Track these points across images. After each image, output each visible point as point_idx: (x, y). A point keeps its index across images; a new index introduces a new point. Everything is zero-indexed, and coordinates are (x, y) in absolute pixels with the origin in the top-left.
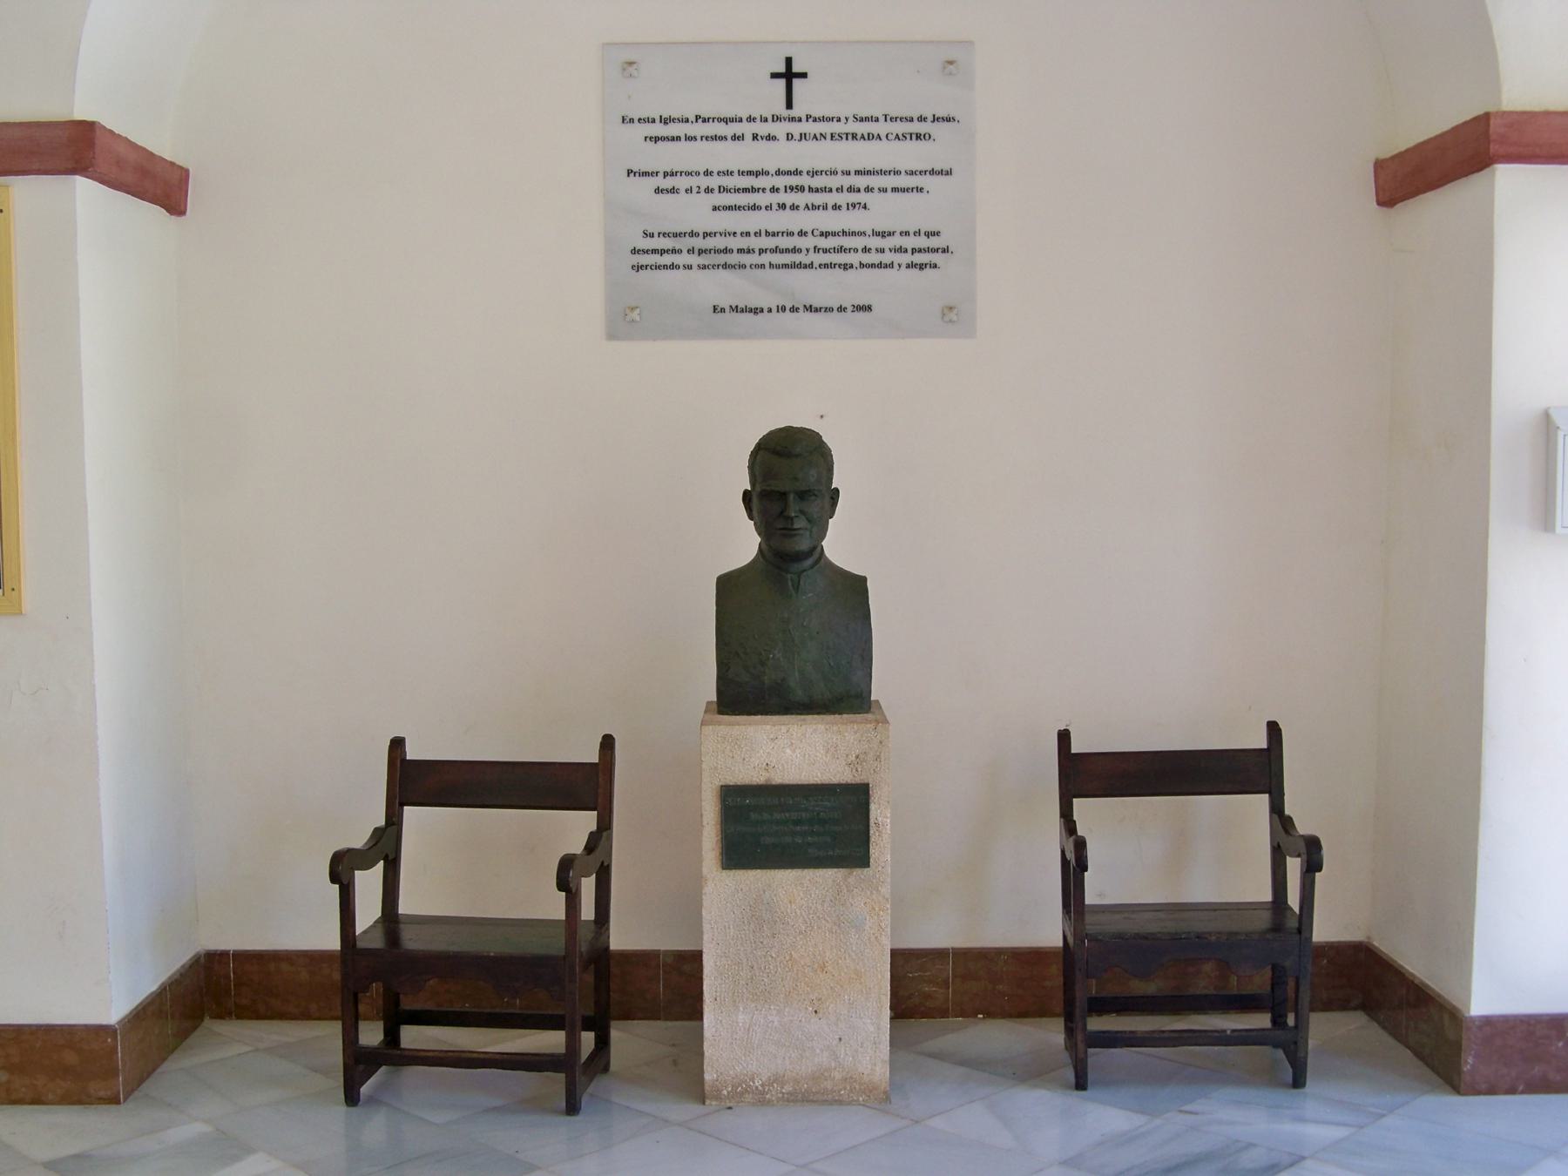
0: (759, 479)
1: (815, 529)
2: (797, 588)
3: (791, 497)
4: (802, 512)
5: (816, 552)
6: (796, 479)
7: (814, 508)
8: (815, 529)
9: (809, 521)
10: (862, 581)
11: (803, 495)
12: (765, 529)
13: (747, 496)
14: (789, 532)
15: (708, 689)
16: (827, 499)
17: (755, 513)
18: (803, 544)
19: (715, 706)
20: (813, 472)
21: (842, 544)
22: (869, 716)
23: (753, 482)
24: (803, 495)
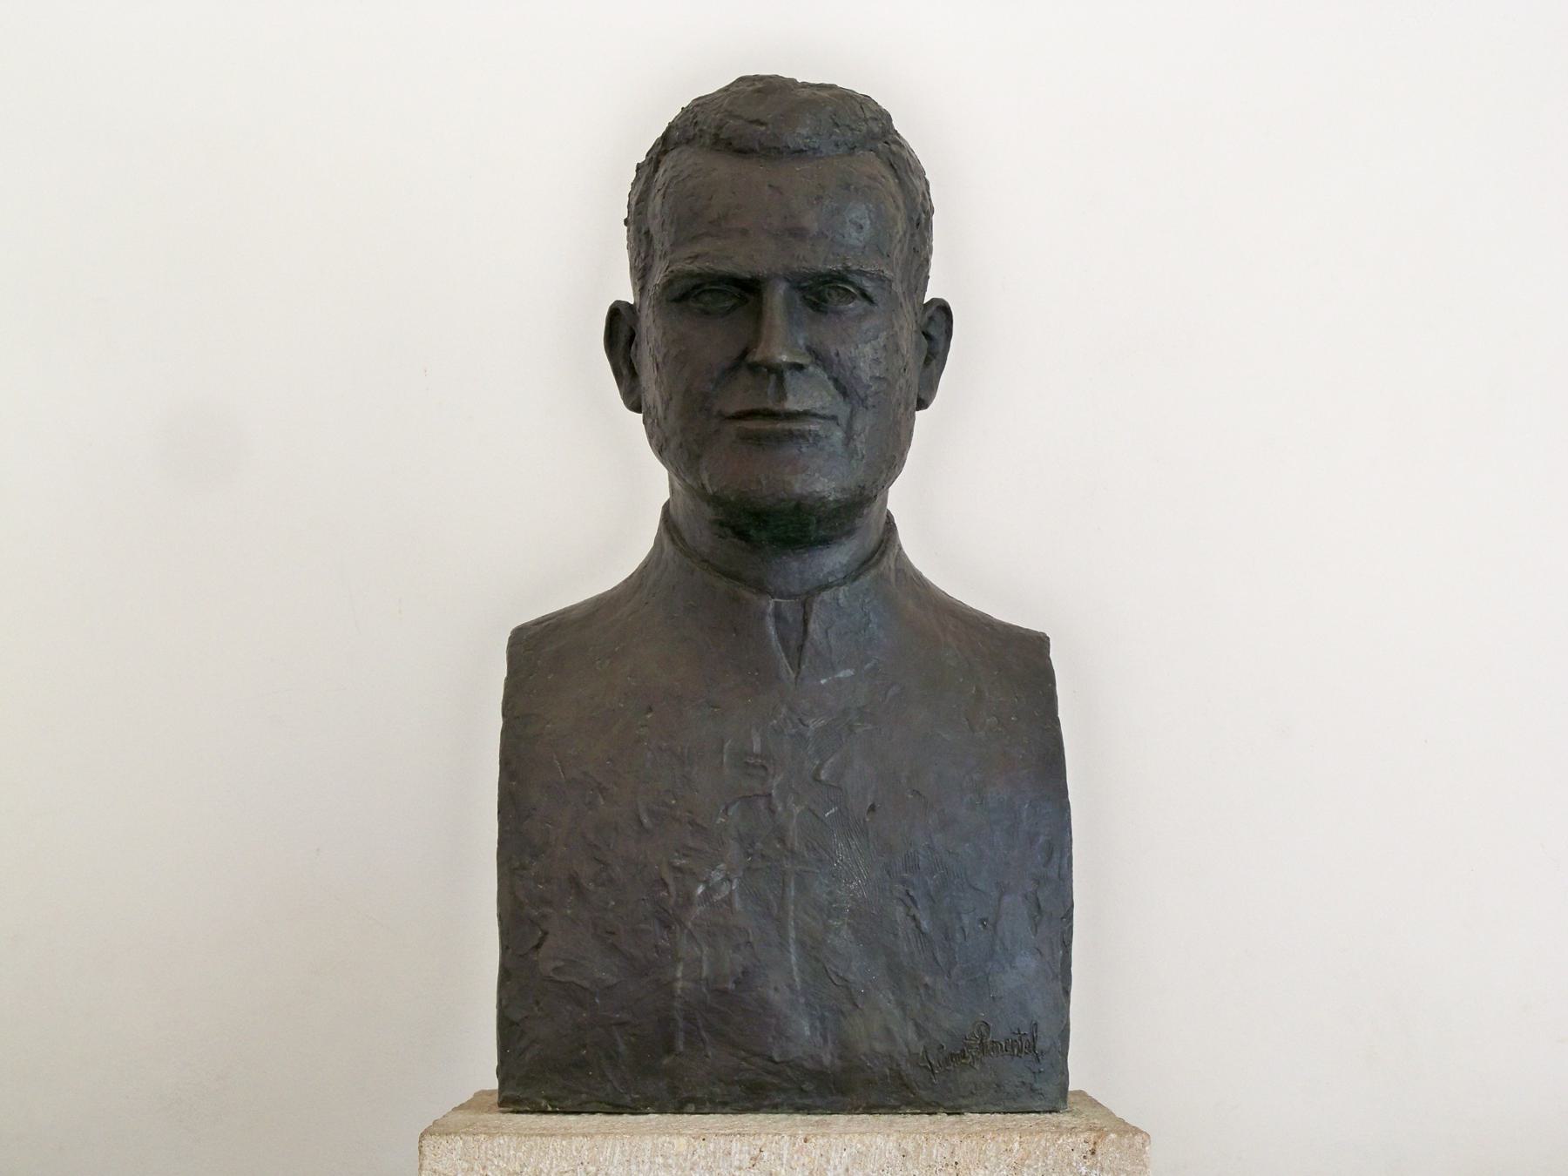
0: (662, 240)
1: (864, 423)
2: (797, 650)
3: (777, 297)
4: (819, 356)
5: (856, 514)
6: (798, 233)
7: (865, 348)
8: (864, 422)
9: (844, 391)
10: (1037, 645)
11: (822, 292)
12: (679, 442)
13: (621, 330)
14: (769, 428)
15: (481, 1066)
16: (908, 338)
17: (651, 388)
18: (822, 481)
19: (496, 1098)
20: (859, 212)
21: (975, 504)
22: (1063, 1118)
23: (641, 273)
24: (822, 292)
